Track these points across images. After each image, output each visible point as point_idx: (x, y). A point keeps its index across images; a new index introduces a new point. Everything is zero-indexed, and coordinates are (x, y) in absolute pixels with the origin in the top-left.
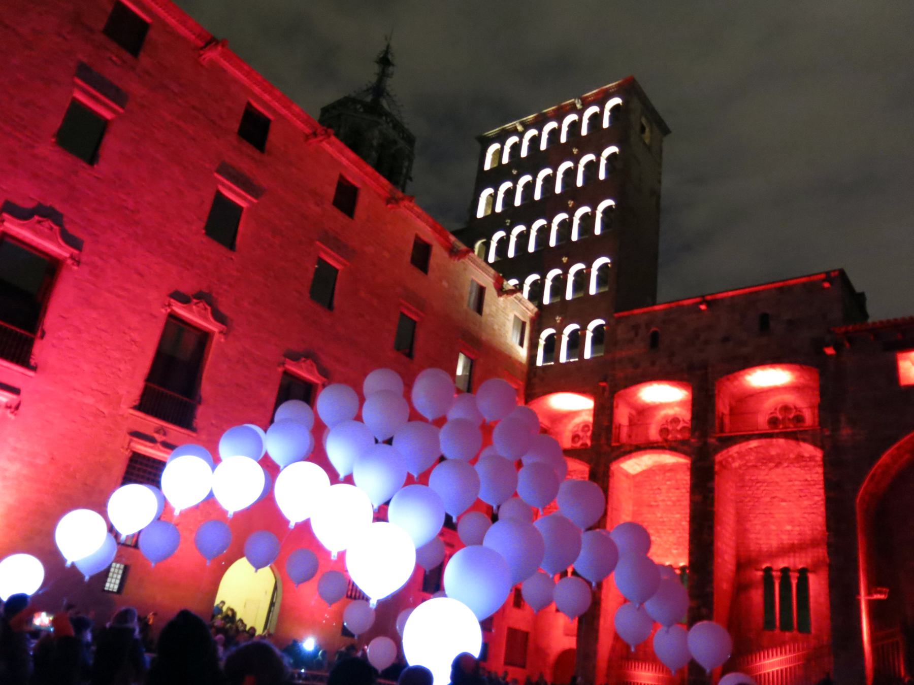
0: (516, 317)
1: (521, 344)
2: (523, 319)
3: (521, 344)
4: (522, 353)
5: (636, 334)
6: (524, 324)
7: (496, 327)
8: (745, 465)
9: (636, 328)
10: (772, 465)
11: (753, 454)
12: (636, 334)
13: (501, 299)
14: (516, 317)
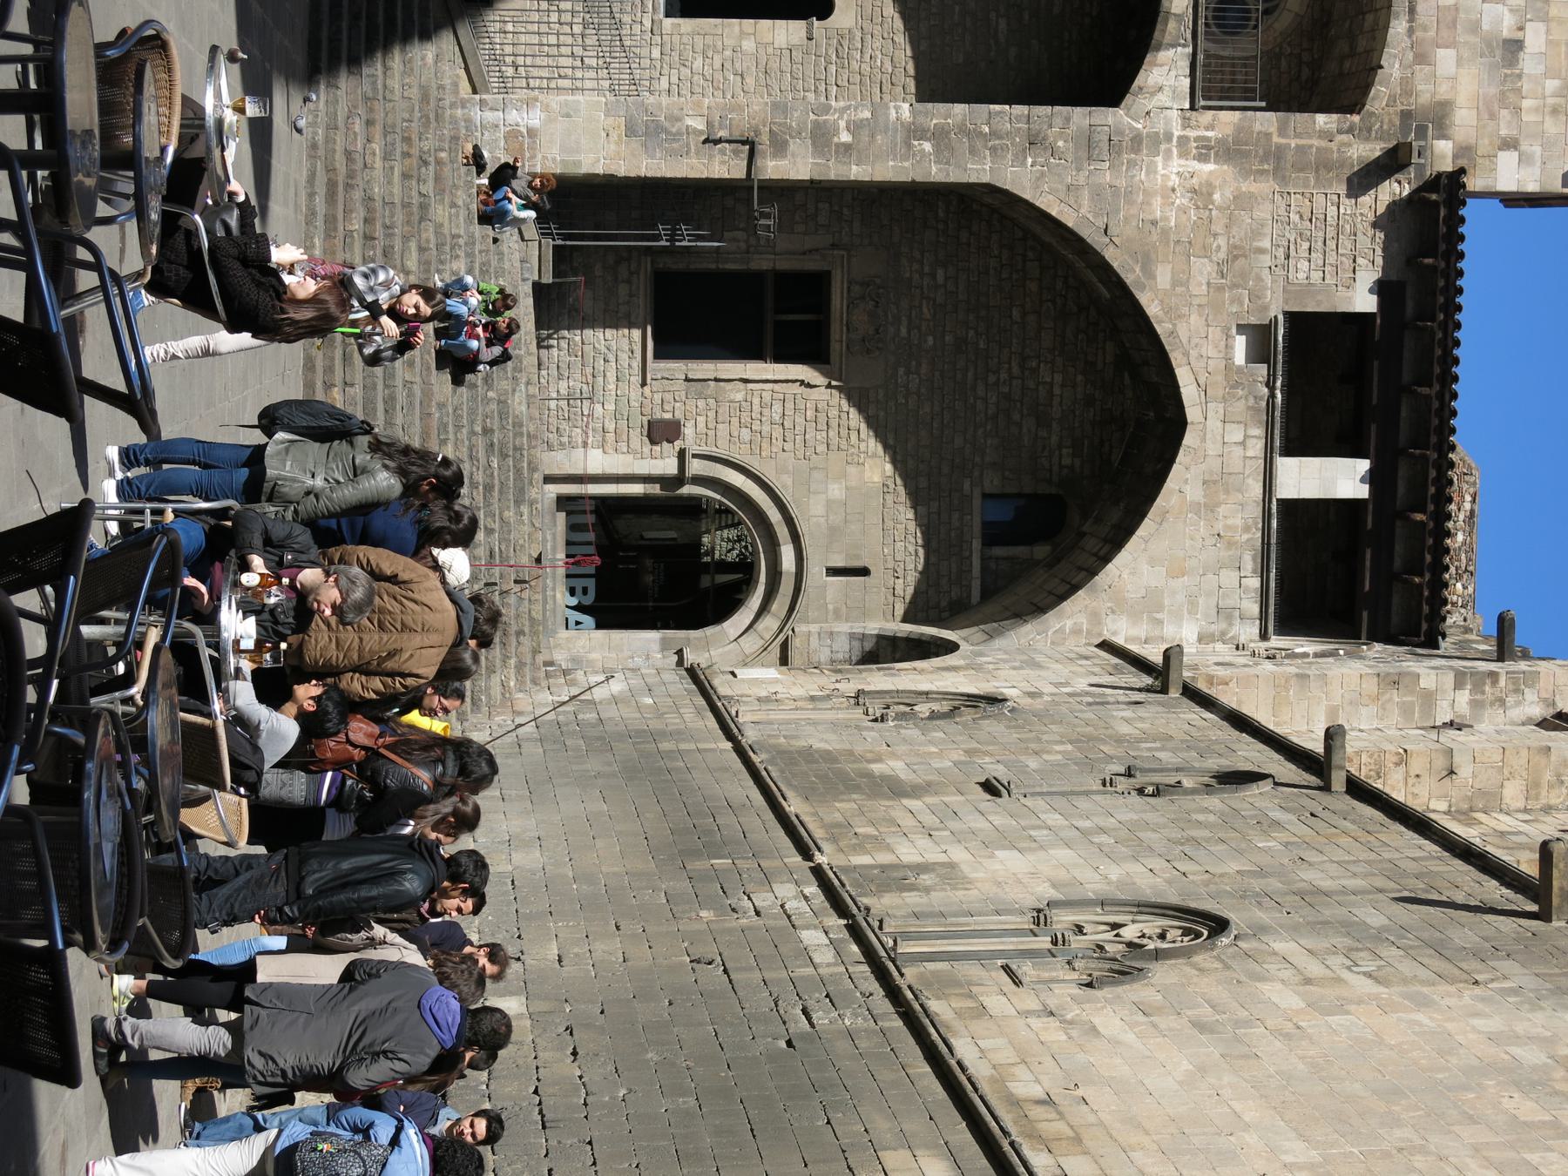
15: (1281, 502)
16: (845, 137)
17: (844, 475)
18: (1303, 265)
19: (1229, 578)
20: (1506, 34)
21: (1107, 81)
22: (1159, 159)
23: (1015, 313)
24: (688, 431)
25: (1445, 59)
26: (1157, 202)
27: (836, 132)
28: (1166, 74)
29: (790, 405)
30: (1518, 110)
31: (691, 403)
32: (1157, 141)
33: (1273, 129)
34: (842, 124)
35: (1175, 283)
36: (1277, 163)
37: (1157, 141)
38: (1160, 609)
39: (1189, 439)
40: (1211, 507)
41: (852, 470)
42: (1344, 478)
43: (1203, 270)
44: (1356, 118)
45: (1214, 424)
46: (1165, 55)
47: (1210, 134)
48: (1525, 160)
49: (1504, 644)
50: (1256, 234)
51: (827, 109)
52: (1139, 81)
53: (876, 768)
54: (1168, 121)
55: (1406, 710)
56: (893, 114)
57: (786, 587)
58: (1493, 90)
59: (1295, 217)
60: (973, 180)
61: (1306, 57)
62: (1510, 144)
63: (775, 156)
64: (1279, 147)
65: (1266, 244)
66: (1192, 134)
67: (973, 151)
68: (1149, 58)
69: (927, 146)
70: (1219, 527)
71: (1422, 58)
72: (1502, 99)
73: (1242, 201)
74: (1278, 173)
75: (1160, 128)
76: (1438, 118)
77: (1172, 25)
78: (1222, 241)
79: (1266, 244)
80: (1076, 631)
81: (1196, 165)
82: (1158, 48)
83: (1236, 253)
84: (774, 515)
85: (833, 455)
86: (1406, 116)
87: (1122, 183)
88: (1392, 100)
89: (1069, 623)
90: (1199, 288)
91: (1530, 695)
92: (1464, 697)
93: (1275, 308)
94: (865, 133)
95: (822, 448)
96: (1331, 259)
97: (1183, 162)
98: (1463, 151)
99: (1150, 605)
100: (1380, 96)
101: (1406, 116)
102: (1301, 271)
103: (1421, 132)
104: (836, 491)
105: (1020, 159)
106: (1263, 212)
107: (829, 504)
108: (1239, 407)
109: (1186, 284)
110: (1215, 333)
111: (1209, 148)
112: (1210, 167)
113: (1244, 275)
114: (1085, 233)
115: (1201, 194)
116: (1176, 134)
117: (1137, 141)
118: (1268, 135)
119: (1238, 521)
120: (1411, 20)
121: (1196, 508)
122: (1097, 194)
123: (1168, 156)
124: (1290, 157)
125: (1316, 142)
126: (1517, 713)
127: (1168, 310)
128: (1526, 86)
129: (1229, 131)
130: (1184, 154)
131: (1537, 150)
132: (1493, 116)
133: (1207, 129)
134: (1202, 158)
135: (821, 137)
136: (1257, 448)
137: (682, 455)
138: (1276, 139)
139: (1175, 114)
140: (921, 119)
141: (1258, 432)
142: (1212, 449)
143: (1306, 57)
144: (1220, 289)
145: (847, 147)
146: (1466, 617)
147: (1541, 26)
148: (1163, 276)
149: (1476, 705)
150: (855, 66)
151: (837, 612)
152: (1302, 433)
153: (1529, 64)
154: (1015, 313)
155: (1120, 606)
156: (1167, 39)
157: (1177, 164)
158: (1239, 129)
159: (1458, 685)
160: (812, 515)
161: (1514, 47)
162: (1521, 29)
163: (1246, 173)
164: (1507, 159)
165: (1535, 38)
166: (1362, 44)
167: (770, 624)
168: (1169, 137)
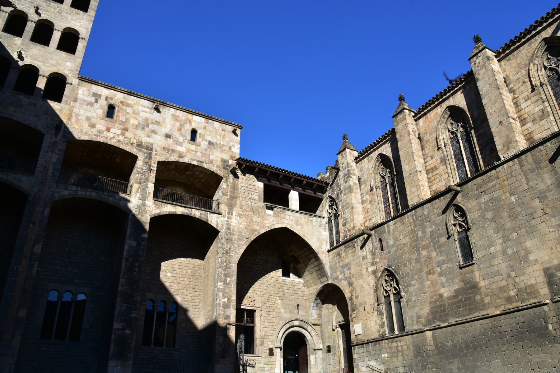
5: (96, 101)
9: (97, 96)
12: (96, 101)
15: (300, 209)
16: (226, 300)
17: (279, 308)
18: (254, 196)
19: (314, 223)
21: (211, 233)
22: (232, 224)
23: (246, 265)
24: (271, 346)
25: (212, 157)
26: (241, 226)
27: (225, 302)
28: (213, 220)
29: (265, 320)
30: (224, 145)
31: (265, 345)
33: (226, 197)
34: (223, 300)
35: (258, 225)
36: (233, 198)
38: (320, 238)
39: (289, 228)
40: (302, 225)
41: (278, 307)
42: (294, 197)
43: (255, 218)
44: (224, 179)
45: (286, 221)
46: (209, 219)
49: (336, 169)
50: (248, 205)
51: (219, 304)
52: (214, 226)
53: (446, 295)
55: (357, 188)
56: (221, 287)
57: (302, 324)
58: (219, 149)
59: (245, 196)
60: (236, 269)
62: (230, 148)
63: (230, 319)
64: (230, 197)
65: (250, 203)
66: (227, 216)
67: (230, 268)
68: (209, 223)
69: (228, 279)
70: (305, 224)
71: (212, 162)
72: (221, 148)
73: (241, 207)
74: (236, 198)
75: (226, 223)
76: (224, 161)
77: (203, 216)
78: (250, 213)
79: (250, 203)
80: (326, 257)
81: (234, 216)
82: (208, 220)
83: (252, 210)
84: (288, 326)
85: (275, 311)
87: (237, 233)
88: (220, 170)
89: (324, 259)
90: (259, 220)
91: (352, 164)
92: (353, 176)
93: (262, 204)
94: (226, 295)
95: (274, 313)
96: (253, 190)
98: (232, 158)
99: (319, 240)
100: (220, 173)
101: (224, 168)
102: (255, 197)
103: (227, 166)
104: (283, 311)
105: (232, 257)
106: (244, 203)
107: (286, 313)
108: (282, 215)
109: (258, 223)
110: (268, 218)
113: (257, 210)
114: (248, 244)
115: (240, 215)
118: (228, 199)
119: (304, 219)
121: (302, 228)
122: (239, 240)
124: (232, 195)
125: (229, 188)
126: (355, 168)
127: (264, 227)
128: (218, 142)
129: (226, 207)
131: (231, 143)
132: (224, 150)
134: (232, 214)
135: (226, 306)
136: (290, 213)
137: (276, 348)
139: (223, 219)
140: (222, 280)
141: (287, 212)
142: (290, 223)
144: (259, 215)
145: (228, 299)
146: (327, 176)
147: (206, 136)
148: (257, 227)
149: (354, 175)
150: (190, 298)
151: (306, 312)
152: (285, 203)
153: (214, 141)
154: (246, 265)
155: (320, 247)
156: (206, 218)
157: (233, 220)
158: (226, 205)
159: (351, 177)
160: (287, 316)
161: (210, 143)
163: (236, 205)
164: (233, 149)
165: (209, 138)
166: (201, 176)
167: (309, 329)
168: (227, 221)
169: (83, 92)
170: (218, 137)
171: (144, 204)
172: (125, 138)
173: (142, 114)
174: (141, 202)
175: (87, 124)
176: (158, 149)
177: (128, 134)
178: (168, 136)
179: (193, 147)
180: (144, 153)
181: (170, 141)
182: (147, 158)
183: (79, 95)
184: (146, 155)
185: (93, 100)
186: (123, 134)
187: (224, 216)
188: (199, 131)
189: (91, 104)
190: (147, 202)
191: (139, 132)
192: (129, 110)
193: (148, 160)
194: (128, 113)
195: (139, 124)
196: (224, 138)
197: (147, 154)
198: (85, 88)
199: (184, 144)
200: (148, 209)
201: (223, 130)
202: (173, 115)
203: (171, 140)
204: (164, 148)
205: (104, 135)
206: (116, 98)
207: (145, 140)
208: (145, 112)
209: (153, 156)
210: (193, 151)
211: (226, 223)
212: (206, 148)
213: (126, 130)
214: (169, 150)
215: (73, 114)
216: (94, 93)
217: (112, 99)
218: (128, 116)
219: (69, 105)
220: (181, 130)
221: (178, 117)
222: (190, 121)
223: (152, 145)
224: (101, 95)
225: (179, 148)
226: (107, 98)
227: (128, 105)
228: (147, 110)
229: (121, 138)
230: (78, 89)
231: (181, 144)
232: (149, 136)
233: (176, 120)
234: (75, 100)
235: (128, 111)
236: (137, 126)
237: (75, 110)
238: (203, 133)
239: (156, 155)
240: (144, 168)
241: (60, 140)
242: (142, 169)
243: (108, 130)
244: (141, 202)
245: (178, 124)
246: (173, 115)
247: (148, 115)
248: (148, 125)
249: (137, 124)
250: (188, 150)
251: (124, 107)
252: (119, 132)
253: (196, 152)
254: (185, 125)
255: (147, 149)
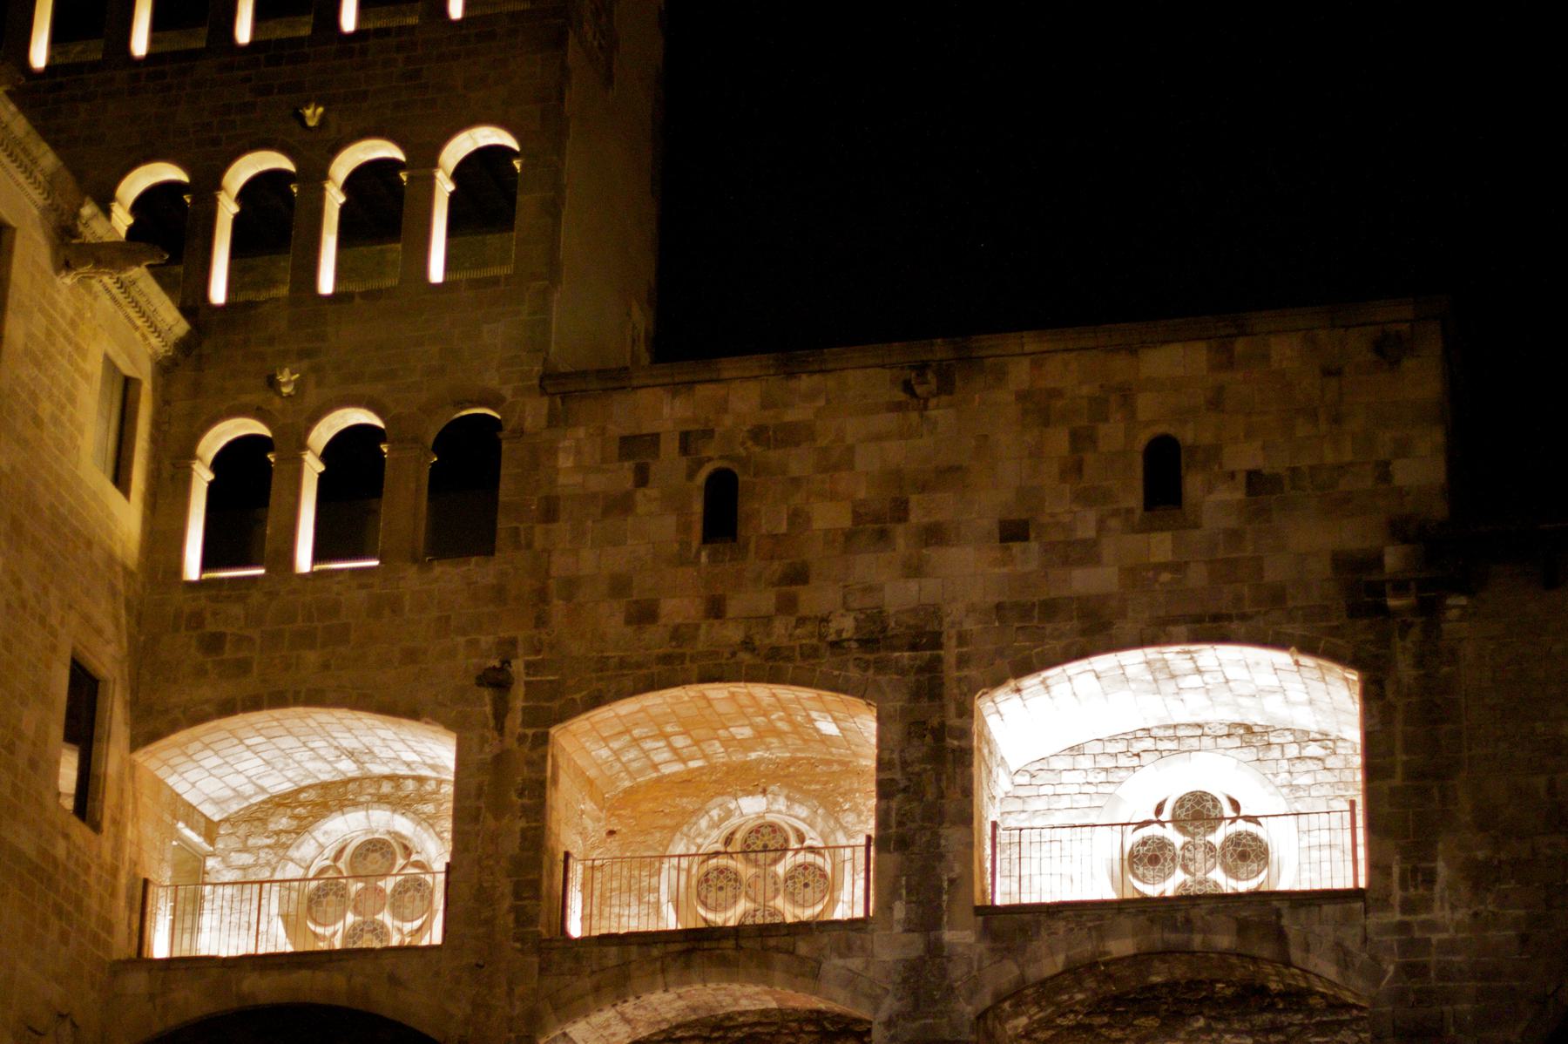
0: (107, 358)
1: (121, 479)
2: (127, 369)
3: (121, 479)
4: (125, 518)
6: (128, 386)
7: (46, 409)
8: (1047, 1023)
10: (1150, 1022)
11: (1090, 983)
13: (68, 280)
14: (107, 358)
20: (1239, 495)
22: (1435, 938)
25: (1277, 570)
26: (1493, 935)
30: (1341, 468)
32: (1411, 944)
37: (1411, 944)
47: (1396, 870)
48: (1403, 449)
54: (1384, 929)
61: (1292, 751)
62: (1384, 472)
65: (1541, 782)
66: (1397, 895)
75: (1392, 939)
86: (1354, 611)
97: (1437, 904)
101: (1354, 611)
111: (1415, 870)
112: (1441, 868)
115: (1479, 877)
116: (1398, 917)
117: (1411, 970)
120: (1229, 618)
123: (1431, 926)
130: (1427, 904)
133: (1390, 875)
134: (1430, 879)
138: (1397, 781)
139: (1373, 920)
143: (1292, 751)
157: (1441, 913)
161: (1256, 482)
162: (1232, 475)
165: (1245, 456)
168: (1404, 927)
169: (578, 452)
170: (1302, 429)
171: (935, 949)
172: (802, 621)
173: (868, 460)
174: (916, 945)
175: (620, 618)
176: (970, 625)
177: (814, 599)
178: (1013, 532)
179: (1161, 546)
180: (902, 672)
181: (1028, 556)
182: (916, 695)
183: (562, 480)
184: (911, 678)
185: (624, 475)
186: (787, 605)
187: (1384, 903)
188: (1186, 435)
189: (621, 505)
190: (948, 936)
191: (870, 566)
192: (799, 462)
193: (925, 703)
194: (795, 482)
195: (857, 517)
196: (1337, 420)
197: (920, 670)
198: (581, 432)
199: (1108, 549)
200: (957, 972)
201: (1328, 373)
202: (1022, 396)
203: (1034, 546)
204: (999, 607)
205: (701, 646)
206: (728, 421)
207: (901, 597)
208: (878, 438)
209: (951, 673)
210: (1164, 567)
211: (1392, 939)
212: (1232, 522)
213: (798, 576)
214: (1025, 611)
215: (553, 584)
216: (624, 440)
217: (708, 434)
218: (797, 500)
219: (529, 546)
220: (1078, 468)
221: (1056, 393)
222: (1126, 395)
223: (935, 612)
224: (655, 438)
225: (1085, 581)
226: (686, 442)
227: (791, 436)
228: (886, 421)
229: (781, 630)
230: (553, 452)
231: (1087, 553)
232: (914, 570)
233: (1046, 419)
234: (550, 512)
235: (795, 469)
236: (849, 536)
237: (560, 565)
238: (1207, 438)
239: (962, 662)
240: (914, 753)
241: (522, 739)
242: (905, 764)
243: (716, 609)
244: (917, 939)
245: (1059, 441)
246: (1022, 396)
247: (895, 453)
248: (900, 511)
249: (846, 522)
250: (1134, 575)
251: (774, 455)
252: (766, 601)
253: (1178, 567)
254: (1103, 429)
255: (914, 647)
